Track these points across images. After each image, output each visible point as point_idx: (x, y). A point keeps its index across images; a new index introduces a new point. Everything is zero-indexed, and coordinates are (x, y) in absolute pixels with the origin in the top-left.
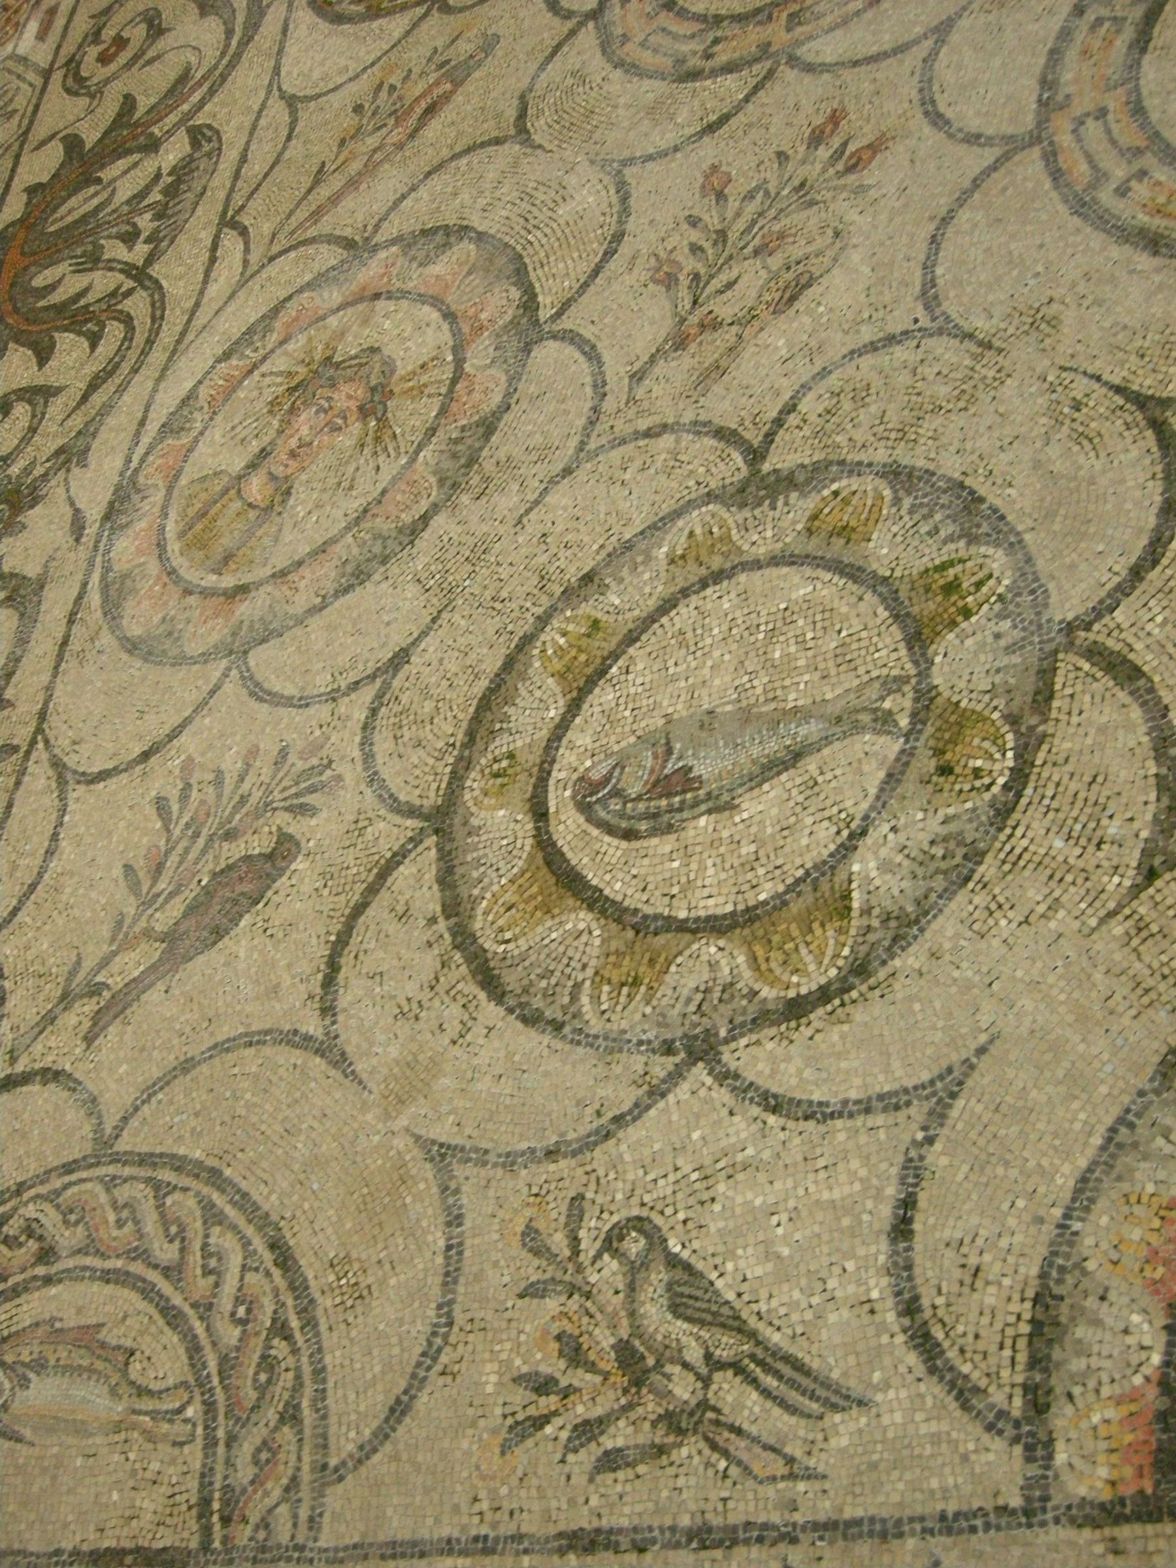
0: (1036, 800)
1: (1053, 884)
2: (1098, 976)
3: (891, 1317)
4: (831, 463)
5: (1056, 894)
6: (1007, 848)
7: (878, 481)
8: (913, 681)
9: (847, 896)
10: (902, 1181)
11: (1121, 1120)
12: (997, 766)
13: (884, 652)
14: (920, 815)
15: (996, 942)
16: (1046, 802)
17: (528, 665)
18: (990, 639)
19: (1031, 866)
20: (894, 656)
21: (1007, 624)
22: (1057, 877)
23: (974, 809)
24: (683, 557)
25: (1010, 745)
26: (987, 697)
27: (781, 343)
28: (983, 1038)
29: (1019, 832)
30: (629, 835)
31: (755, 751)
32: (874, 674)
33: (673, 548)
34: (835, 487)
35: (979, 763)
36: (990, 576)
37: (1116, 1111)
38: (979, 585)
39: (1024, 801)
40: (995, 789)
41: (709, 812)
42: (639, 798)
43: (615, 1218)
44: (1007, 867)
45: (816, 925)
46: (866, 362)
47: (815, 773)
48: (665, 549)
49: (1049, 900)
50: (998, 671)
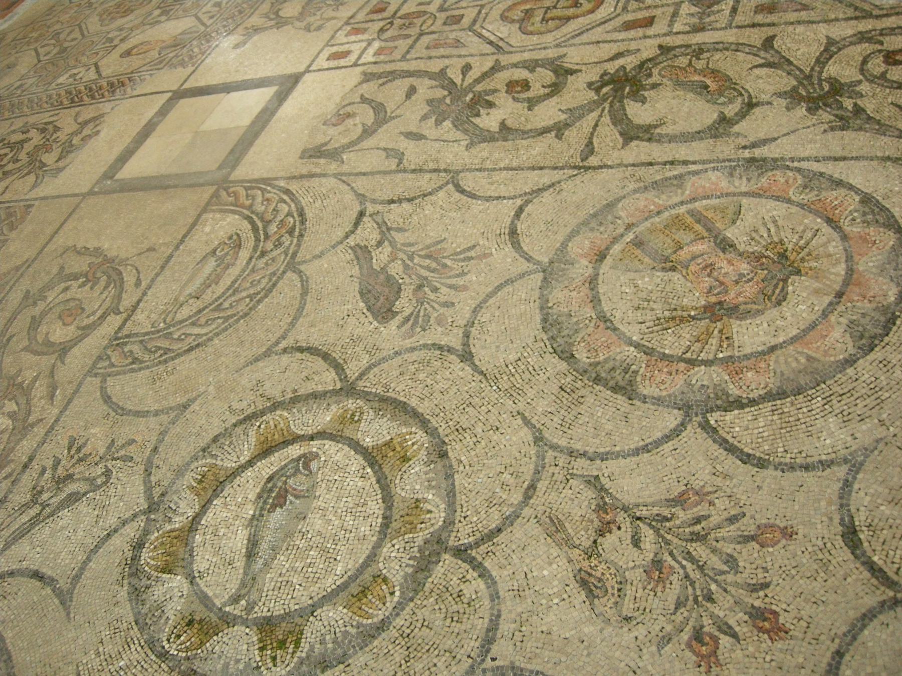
0: (147, 659)
1: (107, 656)
2: (60, 664)
3: (14, 567)
4: (416, 592)
5: (102, 657)
6: (136, 642)
7: (381, 617)
8: (245, 617)
9: (170, 572)
10: (49, 577)
11: (10, 658)
12: (175, 646)
13: (272, 605)
14: (179, 608)
15: (103, 628)
16: (143, 663)
17: (405, 424)
18: (239, 657)
19: (121, 650)
20: (266, 609)
21: (241, 667)
22: (109, 659)
23: (164, 631)
24: (417, 507)
25: (180, 654)
26: (210, 649)
27: (545, 573)
28: (72, 615)
29: (139, 649)
30: (270, 479)
31: (267, 539)
32: (263, 599)
33: (426, 500)
34: (397, 594)
35: (182, 638)
36: (275, 666)
37: (14, 658)
38: (274, 659)
39: (149, 652)
40: (165, 643)
41: (253, 516)
42: (285, 482)
43: (114, 473)
44: (129, 640)
45: (168, 558)
46: (482, 625)
47: (234, 565)
48: (430, 497)
49: (102, 653)
50: (220, 657)
